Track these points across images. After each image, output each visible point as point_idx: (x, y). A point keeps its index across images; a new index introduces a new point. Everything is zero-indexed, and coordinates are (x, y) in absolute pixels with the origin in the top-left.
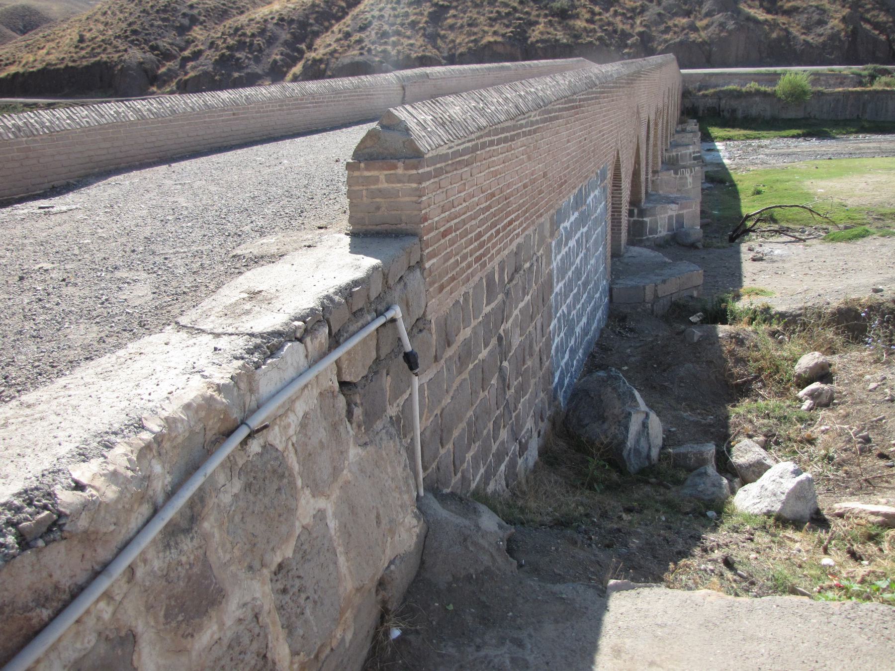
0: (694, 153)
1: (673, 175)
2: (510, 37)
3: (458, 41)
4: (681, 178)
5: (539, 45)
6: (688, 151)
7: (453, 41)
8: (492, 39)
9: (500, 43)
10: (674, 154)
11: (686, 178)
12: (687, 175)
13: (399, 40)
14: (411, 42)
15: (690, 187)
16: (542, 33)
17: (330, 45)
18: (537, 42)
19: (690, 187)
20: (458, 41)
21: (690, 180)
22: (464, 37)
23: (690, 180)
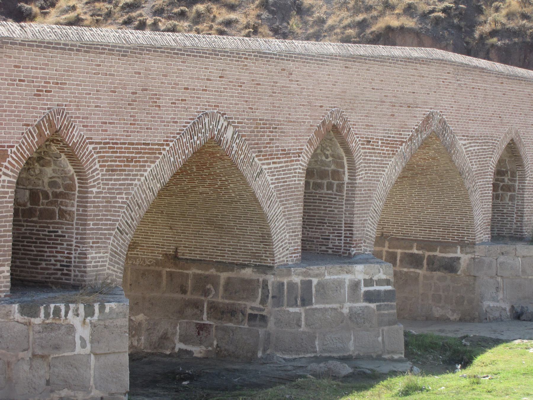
0: (369, 282)
1: (17, 316)
2: (437, 20)
3: (330, 22)
4: (47, 327)
5: (495, 40)
6: (347, 278)
7: (322, 21)
8: (395, 23)
9: (410, 30)
10: (297, 279)
11: (71, 329)
12: (76, 321)
13: (209, 10)
14: (233, 16)
15: (78, 350)
16: (510, 16)
17: (74, 8)
18: (493, 33)
19: (78, 350)
20: (330, 22)
21: (82, 332)
22: (344, 14)
23: (82, 332)
